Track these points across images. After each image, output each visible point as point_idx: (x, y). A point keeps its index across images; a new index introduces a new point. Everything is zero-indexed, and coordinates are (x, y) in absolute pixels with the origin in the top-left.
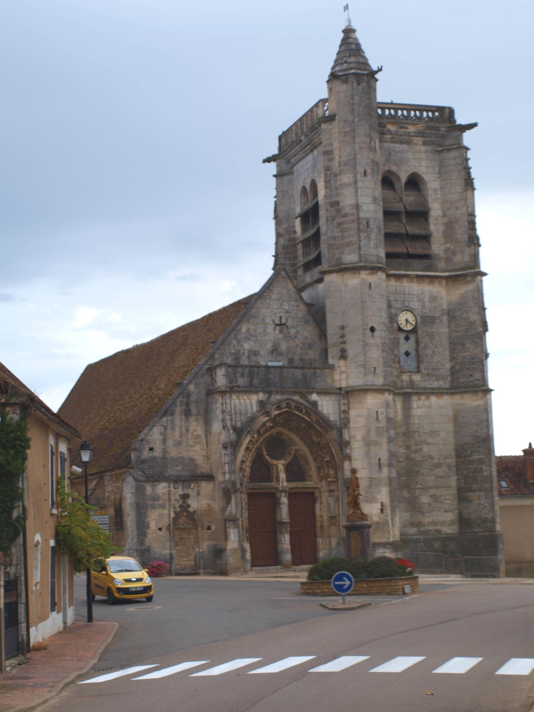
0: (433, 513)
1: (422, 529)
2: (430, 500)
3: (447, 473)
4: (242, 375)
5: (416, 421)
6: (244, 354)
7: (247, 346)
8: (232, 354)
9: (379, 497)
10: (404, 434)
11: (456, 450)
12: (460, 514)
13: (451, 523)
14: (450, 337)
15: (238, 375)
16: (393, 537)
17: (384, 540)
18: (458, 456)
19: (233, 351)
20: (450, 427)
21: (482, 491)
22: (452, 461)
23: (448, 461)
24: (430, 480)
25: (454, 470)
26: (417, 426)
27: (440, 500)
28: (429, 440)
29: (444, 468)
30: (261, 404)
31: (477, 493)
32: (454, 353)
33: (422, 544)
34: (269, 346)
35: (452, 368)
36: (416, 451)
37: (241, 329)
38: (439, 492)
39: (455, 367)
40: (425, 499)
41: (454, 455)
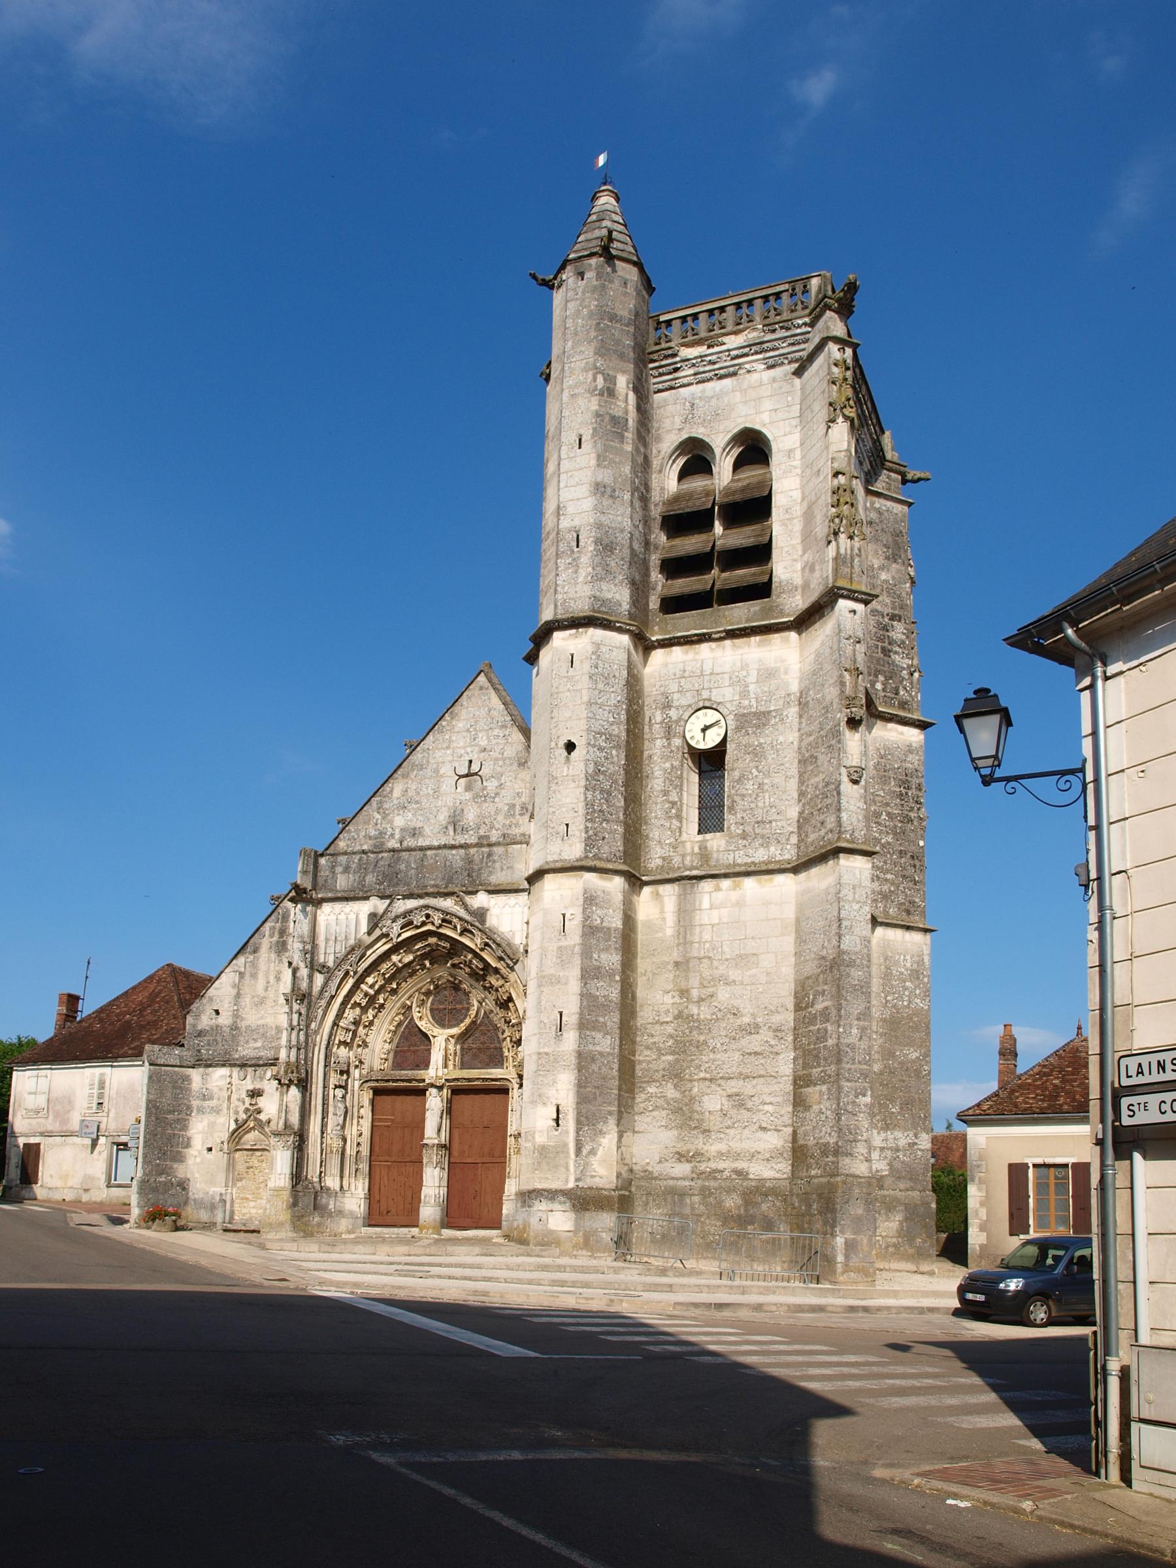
0: (731, 1132)
2: (727, 1104)
3: (772, 1046)
4: (347, 869)
5: (707, 937)
6: (392, 835)
7: (399, 821)
8: (370, 838)
9: (551, 1092)
10: (677, 964)
13: (776, 1154)
15: (339, 869)
16: (577, 1180)
17: (555, 1185)
19: (373, 833)
22: (787, 1018)
23: (777, 1019)
24: (730, 1060)
25: (790, 1038)
26: (707, 945)
28: (734, 974)
29: (765, 1035)
30: (375, 920)
33: (696, 1199)
34: (443, 817)
37: (391, 791)
38: (748, 1088)
40: (712, 1102)
41: (791, 1007)
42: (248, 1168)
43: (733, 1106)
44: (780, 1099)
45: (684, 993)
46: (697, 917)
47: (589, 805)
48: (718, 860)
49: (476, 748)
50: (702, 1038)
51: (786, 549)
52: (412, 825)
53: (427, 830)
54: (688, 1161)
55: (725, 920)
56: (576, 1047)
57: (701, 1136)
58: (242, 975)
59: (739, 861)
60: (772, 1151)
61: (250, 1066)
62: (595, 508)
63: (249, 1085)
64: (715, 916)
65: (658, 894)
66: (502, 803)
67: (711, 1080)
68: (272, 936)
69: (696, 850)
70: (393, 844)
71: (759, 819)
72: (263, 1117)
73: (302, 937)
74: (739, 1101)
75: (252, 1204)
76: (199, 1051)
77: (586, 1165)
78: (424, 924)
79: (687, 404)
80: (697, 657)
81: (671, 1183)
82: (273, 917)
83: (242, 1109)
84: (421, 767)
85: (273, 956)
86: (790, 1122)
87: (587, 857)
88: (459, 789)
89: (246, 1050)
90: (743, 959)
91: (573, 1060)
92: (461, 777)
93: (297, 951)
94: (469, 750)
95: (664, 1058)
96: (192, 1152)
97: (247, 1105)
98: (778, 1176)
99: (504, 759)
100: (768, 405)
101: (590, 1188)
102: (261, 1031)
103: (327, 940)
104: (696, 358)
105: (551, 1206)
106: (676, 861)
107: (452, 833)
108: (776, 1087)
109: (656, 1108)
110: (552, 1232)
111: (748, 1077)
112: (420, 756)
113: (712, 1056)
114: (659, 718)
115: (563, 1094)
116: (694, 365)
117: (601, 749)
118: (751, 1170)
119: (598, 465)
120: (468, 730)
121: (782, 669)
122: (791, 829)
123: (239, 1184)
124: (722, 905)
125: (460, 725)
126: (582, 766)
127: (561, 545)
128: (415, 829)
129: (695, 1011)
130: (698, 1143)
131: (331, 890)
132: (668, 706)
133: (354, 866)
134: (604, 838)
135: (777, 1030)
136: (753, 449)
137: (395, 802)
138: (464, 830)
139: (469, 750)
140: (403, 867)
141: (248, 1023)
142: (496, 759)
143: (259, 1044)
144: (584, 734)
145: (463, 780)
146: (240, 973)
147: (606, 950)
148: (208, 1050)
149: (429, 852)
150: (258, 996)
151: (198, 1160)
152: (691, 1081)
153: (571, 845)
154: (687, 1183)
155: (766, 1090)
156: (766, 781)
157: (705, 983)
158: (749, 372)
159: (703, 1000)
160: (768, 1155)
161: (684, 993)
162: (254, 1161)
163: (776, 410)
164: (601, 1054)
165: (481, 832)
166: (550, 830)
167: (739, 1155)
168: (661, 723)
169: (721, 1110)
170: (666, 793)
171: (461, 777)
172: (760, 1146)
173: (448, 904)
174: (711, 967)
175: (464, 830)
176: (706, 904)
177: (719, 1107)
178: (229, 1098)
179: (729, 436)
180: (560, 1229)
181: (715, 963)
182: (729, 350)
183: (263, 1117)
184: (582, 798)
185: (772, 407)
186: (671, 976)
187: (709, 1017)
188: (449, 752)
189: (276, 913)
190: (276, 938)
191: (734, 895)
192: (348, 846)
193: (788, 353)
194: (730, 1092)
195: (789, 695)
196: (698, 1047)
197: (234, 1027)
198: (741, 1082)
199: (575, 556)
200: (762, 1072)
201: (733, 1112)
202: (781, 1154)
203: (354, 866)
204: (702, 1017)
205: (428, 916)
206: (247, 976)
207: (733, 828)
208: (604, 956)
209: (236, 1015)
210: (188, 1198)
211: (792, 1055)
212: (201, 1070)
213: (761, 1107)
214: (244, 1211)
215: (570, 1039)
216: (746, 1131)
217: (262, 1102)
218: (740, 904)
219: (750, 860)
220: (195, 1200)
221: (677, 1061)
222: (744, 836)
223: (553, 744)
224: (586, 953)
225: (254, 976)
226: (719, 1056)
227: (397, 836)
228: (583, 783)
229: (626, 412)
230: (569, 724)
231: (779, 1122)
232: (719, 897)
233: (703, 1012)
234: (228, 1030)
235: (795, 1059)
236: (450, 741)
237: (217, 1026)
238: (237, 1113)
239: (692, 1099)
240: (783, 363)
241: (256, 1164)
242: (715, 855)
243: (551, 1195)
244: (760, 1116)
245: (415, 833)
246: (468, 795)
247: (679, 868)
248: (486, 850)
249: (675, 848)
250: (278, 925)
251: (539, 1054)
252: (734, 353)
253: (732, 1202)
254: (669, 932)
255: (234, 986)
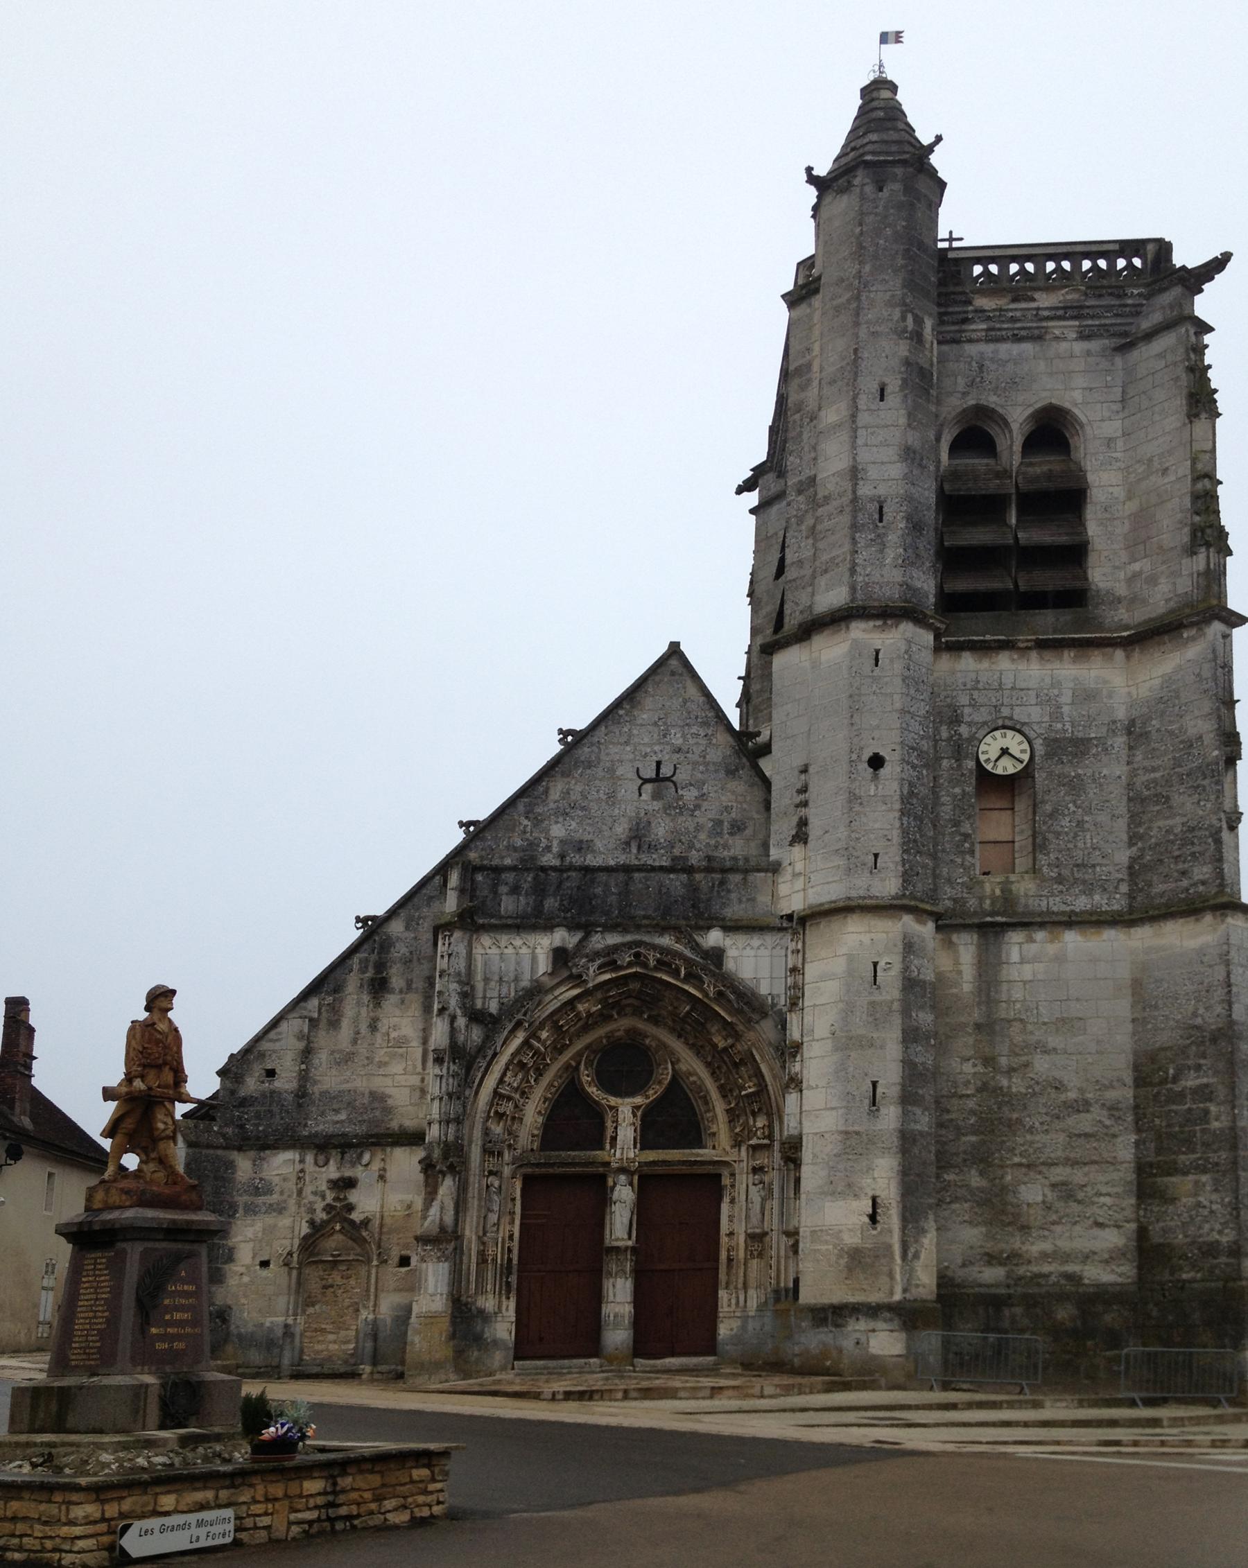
0: (1058, 1229)
1: (1021, 1271)
2: (1050, 1196)
3: (1107, 1127)
4: (515, 890)
5: (1018, 994)
6: (548, 848)
7: (557, 831)
8: (515, 849)
10: (978, 1027)
11: (1136, 1068)
12: (1142, 1233)
14: (1130, 786)
15: (503, 889)
16: (905, 1291)
17: (874, 1298)
18: (1141, 1081)
19: (519, 843)
20: (1123, 1007)
21: (1204, 1171)
23: (1112, 1095)
24: (1053, 1143)
25: (1130, 1118)
26: (1018, 1006)
27: (1080, 1195)
28: (1053, 1041)
29: (1097, 1113)
30: (560, 956)
31: (1191, 1177)
32: (1140, 824)
34: (622, 829)
35: (1133, 860)
36: (1011, 1070)
37: (546, 792)
38: (1078, 1176)
39: (1141, 857)
40: (1032, 1193)
41: (1129, 1080)
42: (325, 1287)
43: (1060, 1198)
44: (1119, 1190)
45: (989, 1061)
46: (1004, 972)
47: (905, 832)
48: (1026, 905)
49: (668, 748)
50: (1015, 1116)
51: (1106, 553)
52: (577, 836)
53: (599, 844)
54: (1001, 1264)
55: (1040, 977)
56: (898, 1125)
57: (1017, 1233)
58: (313, 1023)
59: (1055, 909)
60: (1111, 1251)
61: (335, 1147)
62: (905, 477)
63: (332, 1171)
64: (1027, 971)
65: (951, 942)
66: (705, 817)
67: (1029, 1166)
68: (363, 970)
69: (998, 892)
70: (549, 860)
71: (1080, 861)
72: (356, 1216)
73: (459, 974)
74: (1066, 1191)
75: (331, 1337)
76: (242, 1127)
77: (912, 1270)
78: (630, 965)
79: (974, 364)
80: (994, 667)
81: (982, 1290)
82: (366, 946)
83: (319, 1205)
84: (589, 765)
85: (366, 998)
86: (1133, 1216)
87: (904, 895)
88: (644, 797)
89: (321, 1124)
90: (1064, 1024)
91: (895, 1141)
92: (646, 781)
93: (453, 994)
94: (656, 748)
95: (964, 1139)
96: (236, 1268)
97: (329, 1199)
98: (1120, 1280)
99: (707, 764)
100: (1080, 381)
101: (915, 1300)
102: (346, 1098)
103: (487, 980)
104: (994, 310)
105: (872, 1324)
106: (972, 903)
107: (634, 851)
108: (1116, 1176)
109: (956, 1199)
110: (875, 1357)
111: (1077, 1163)
112: (586, 750)
113: (1029, 1137)
114: (945, 735)
115: (882, 1183)
116: (989, 318)
117: (914, 767)
118: (1086, 1274)
119: (909, 425)
120: (655, 724)
121: (1105, 692)
122: (1120, 876)
123: (310, 1310)
124: (1035, 960)
125: (645, 716)
126: (895, 786)
127: (860, 515)
128: (581, 841)
129: (1005, 1083)
130: (1016, 1243)
131: (492, 916)
132: (956, 720)
133: (525, 886)
134: (918, 874)
135: (1111, 1108)
136: (1051, 431)
137: (552, 805)
138: (652, 848)
139: (656, 748)
140: (599, 890)
141: (325, 1087)
142: (695, 764)
143: (343, 1116)
144: (897, 747)
145: (648, 788)
146: (311, 1020)
147: (922, 1008)
148: (258, 1125)
149: (636, 875)
150: (340, 1051)
151: (246, 1279)
152: (1002, 1167)
153: (883, 880)
154: (1003, 1291)
155: (1101, 1178)
156: (1086, 818)
157: (1017, 1050)
158: (1057, 338)
159: (1014, 1070)
160: (1106, 1256)
161: (989, 1062)
162: (336, 1278)
163: (1091, 389)
164: (921, 1133)
165: (676, 852)
166: (853, 860)
167: (1069, 1255)
168: (950, 738)
169: (1044, 1202)
170: (957, 824)
171: (646, 781)
172: (1097, 1245)
173: (666, 941)
174: (1024, 1031)
175: (652, 848)
176: (1015, 956)
177: (1040, 1198)
178: (300, 1192)
179: (1030, 410)
180: (886, 1353)
181: (1030, 1027)
182: (1038, 309)
183: (356, 1216)
184: (897, 824)
185: (1085, 385)
186: (971, 1040)
187: (1023, 1091)
188: (628, 748)
189: (371, 941)
190: (370, 974)
191: (1052, 949)
192: (482, 858)
193: (1112, 325)
194: (1053, 1180)
195: (1114, 722)
196: (1009, 1126)
197: (302, 1094)
198: (1068, 1170)
199: (881, 531)
200: (1094, 1158)
201: (1059, 1205)
202: (1124, 1254)
203: (525, 886)
204: (1014, 1090)
205: (637, 955)
206: (323, 1024)
207: (1045, 869)
208: (921, 1015)
209: (304, 1077)
210: (228, 1334)
211: (1133, 1138)
212: (252, 1154)
213: (1095, 1199)
214: (319, 1347)
215: (890, 1116)
216: (1078, 1228)
217: (353, 1196)
218: (1060, 959)
219: (1068, 909)
220: (240, 1336)
221: (983, 1142)
222: (1060, 880)
223: (854, 757)
224: (906, 1012)
225: (334, 1024)
226: (1037, 1138)
227: (555, 849)
228: (898, 806)
229: (932, 365)
230: (876, 734)
231: (1117, 1216)
232: (1032, 949)
233: (1017, 1085)
234: (290, 1098)
235: (1137, 1144)
236: (630, 735)
237: (273, 1092)
238: (312, 1211)
239: (1004, 1189)
240: (1102, 335)
241: (339, 1281)
242: (1023, 901)
243: (873, 1311)
244: (1095, 1209)
245: (582, 847)
246: (657, 805)
247: (975, 913)
248: (718, 876)
249: (970, 889)
250: (374, 957)
251: (847, 1133)
252: (1046, 313)
253: (1064, 1313)
254: (967, 987)
255: (300, 1036)
